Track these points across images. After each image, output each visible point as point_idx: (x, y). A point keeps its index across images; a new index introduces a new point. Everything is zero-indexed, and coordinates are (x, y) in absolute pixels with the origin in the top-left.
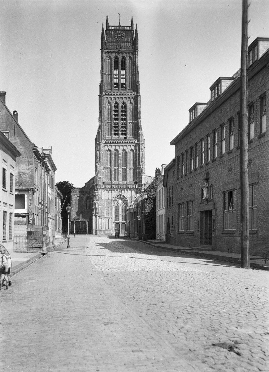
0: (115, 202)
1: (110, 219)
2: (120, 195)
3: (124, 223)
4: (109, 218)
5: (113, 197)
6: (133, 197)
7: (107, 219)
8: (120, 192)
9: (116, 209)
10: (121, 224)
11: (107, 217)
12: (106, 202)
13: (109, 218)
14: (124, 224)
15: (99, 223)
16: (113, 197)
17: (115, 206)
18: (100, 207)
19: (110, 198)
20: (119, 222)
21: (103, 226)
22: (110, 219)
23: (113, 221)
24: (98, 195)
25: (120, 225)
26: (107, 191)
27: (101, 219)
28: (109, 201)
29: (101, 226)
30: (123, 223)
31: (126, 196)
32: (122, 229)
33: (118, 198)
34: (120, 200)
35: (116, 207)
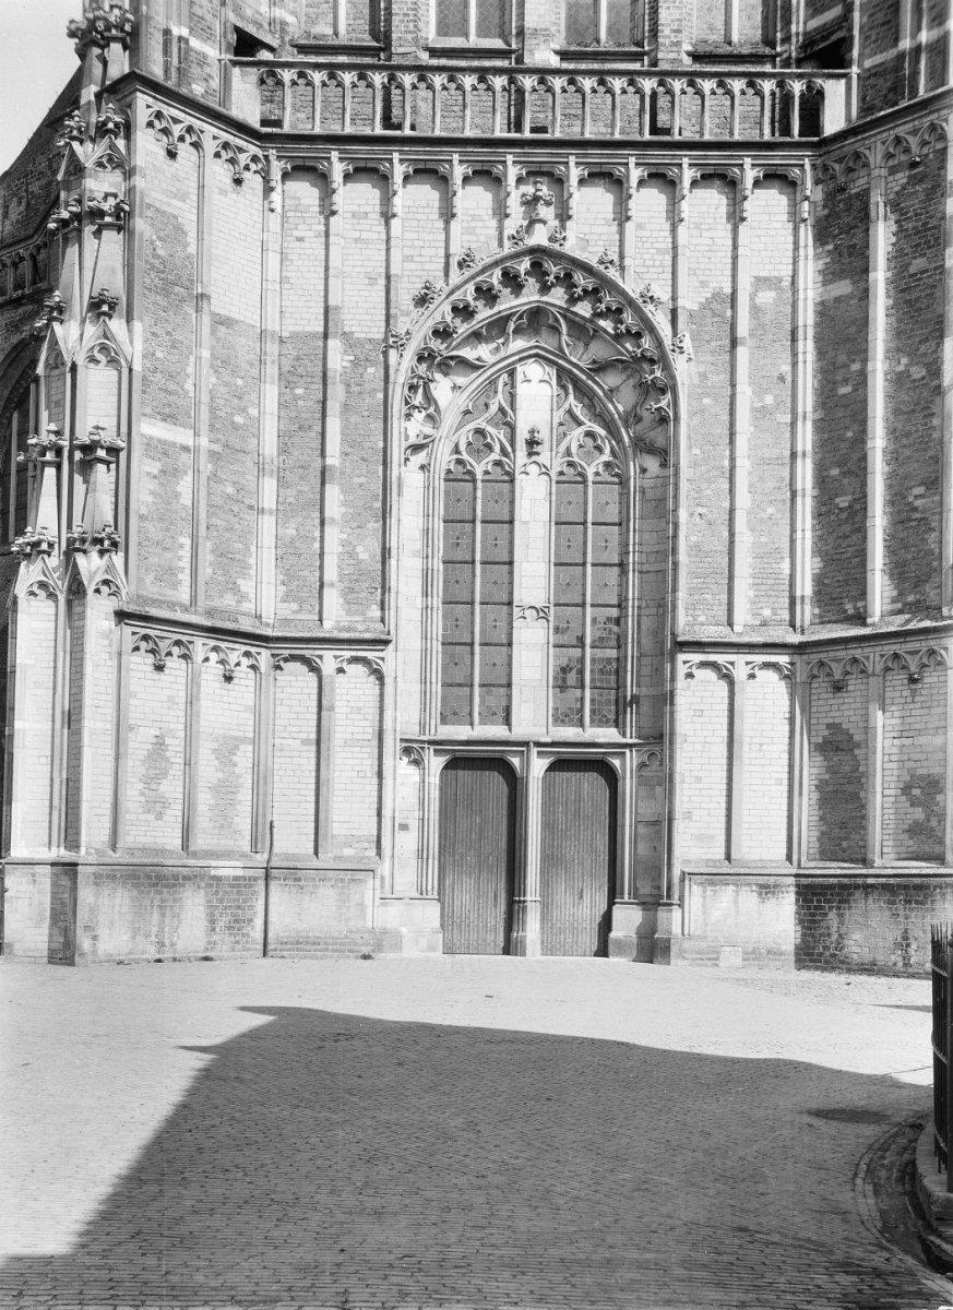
0: (442, 388)
1: (351, 689)
2: (537, 269)
3: (598, 765)
4: (329, 660)
5: (404, 296)
6: (766, 297)
7: (297, 680)
8: (531, 202)
9: (458, 522)
10: (539, 766)
11: (296, 649)
12: (287, 380)
13: (329, 660)
14: (591, 783)
15: (138, 745)
16: (404, 296)
17: (443, 458)
18: (161, 449)
19: (363, 317)
20: (497, 731)
21: (225, 790)
22: (351, 689)
23: (406, 717)
24: (122, 219)
25: (515, 784)
26: (305, 192)
27: (174, 664)
28: (338, 360)
29: (172, 788)
30: (567, 762)
31: (641, 276)
32: (550, 860)
33: (498, 326)
34: (533, 370)
35: (461, 476)
